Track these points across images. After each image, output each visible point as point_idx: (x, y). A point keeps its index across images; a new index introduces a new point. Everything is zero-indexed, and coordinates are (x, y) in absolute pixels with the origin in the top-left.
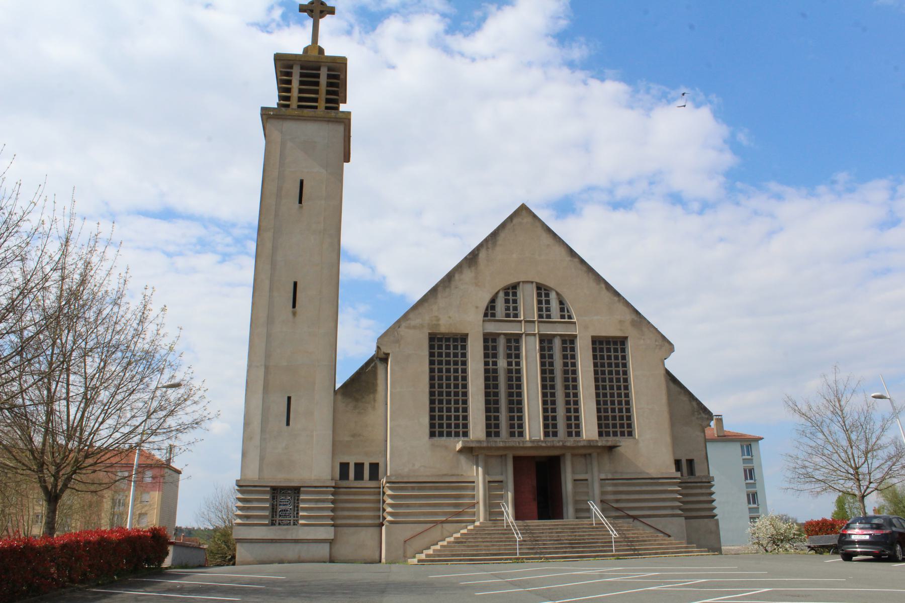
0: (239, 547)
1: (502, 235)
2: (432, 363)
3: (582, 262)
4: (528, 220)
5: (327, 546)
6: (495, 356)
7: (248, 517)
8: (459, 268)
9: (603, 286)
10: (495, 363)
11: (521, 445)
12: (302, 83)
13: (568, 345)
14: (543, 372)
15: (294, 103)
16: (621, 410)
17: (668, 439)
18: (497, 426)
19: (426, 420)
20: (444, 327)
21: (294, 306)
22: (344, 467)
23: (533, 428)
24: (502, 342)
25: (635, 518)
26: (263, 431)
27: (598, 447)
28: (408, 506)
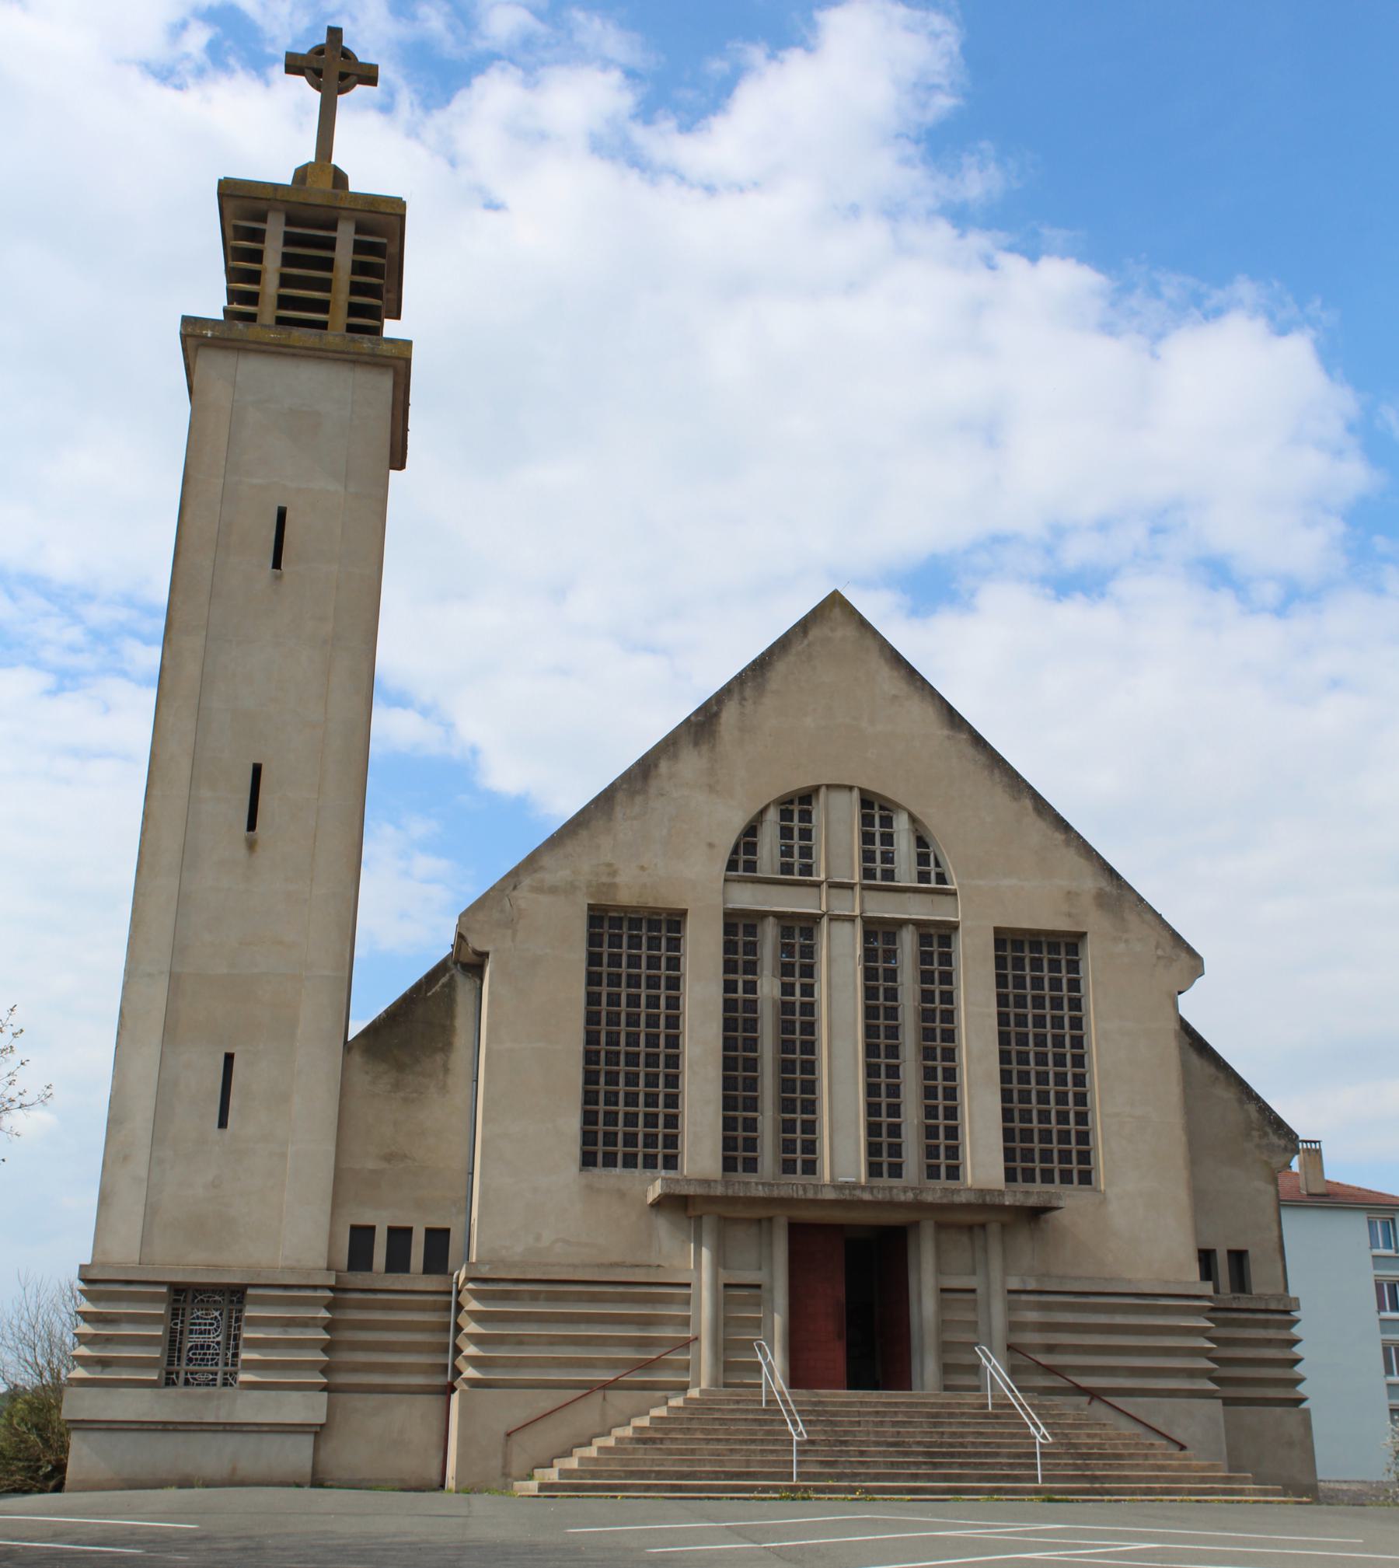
0: (75, 1441)
1: (780, 667)
2: (593, 979)
3: (978, 741)
4: (845, 632)
5: (308, 1441)
6: (751, 968)
7: (104, 1363)
8: (668, 746)
9: (1028, 803)
10: (751, 987)
11: (810, 1195)
12: (288, 260)
13: (935, 948)
14: (870, 1012)
15: (268, 310)
16: (1063, 1118)
17: (1183, 1196)
18: (751, 1144)
19: (572, 1124)
20: (628, 892)
21: (252, 825)
22: (362, 1236)
23: (842, 1156)
24: (769, 936)
25: (1093, 1394)
26: (157, 1139)
27: (1002, 1208)
28: (519, 1341)
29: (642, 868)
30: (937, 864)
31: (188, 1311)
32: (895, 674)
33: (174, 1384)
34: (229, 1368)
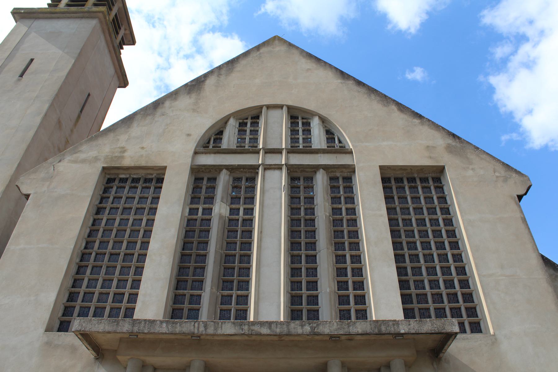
6: (210, 199)
10: (208, 211)
29: (143, 148)
30: (340, 142)
32: (309, 61)
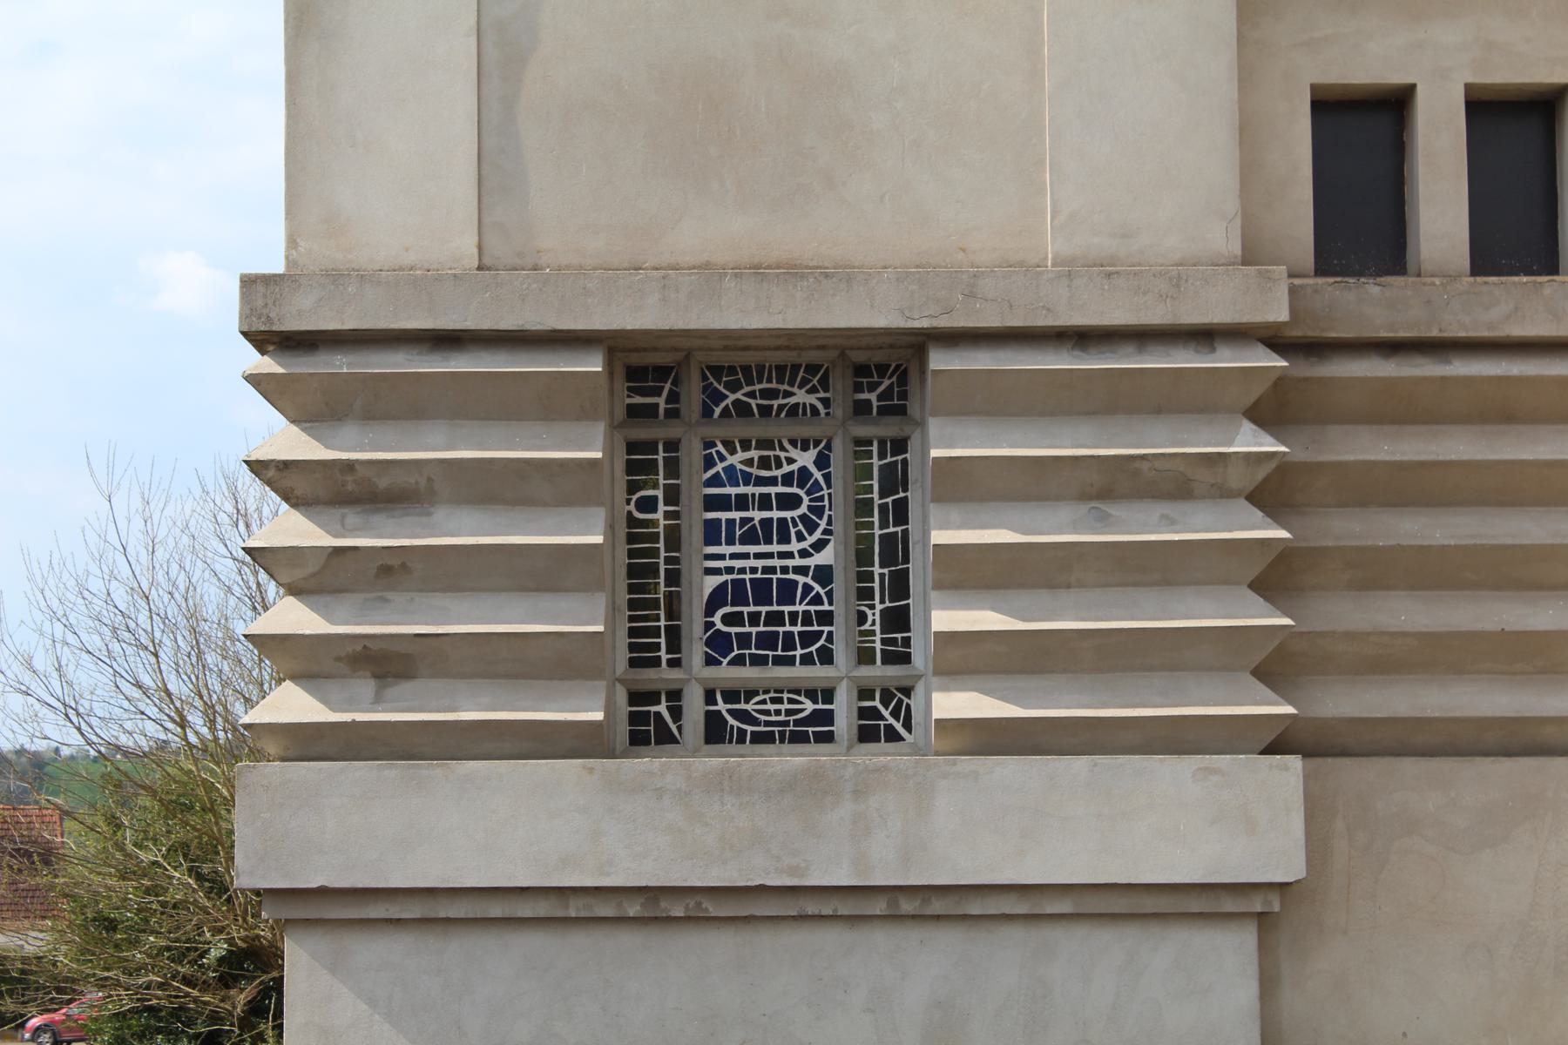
0: (302, 965)
5: (1230, 955)
7: (384, 663)
22: (1361, 130)
31: (692, 453)
33: (666, 737)
34: (879, 672)
